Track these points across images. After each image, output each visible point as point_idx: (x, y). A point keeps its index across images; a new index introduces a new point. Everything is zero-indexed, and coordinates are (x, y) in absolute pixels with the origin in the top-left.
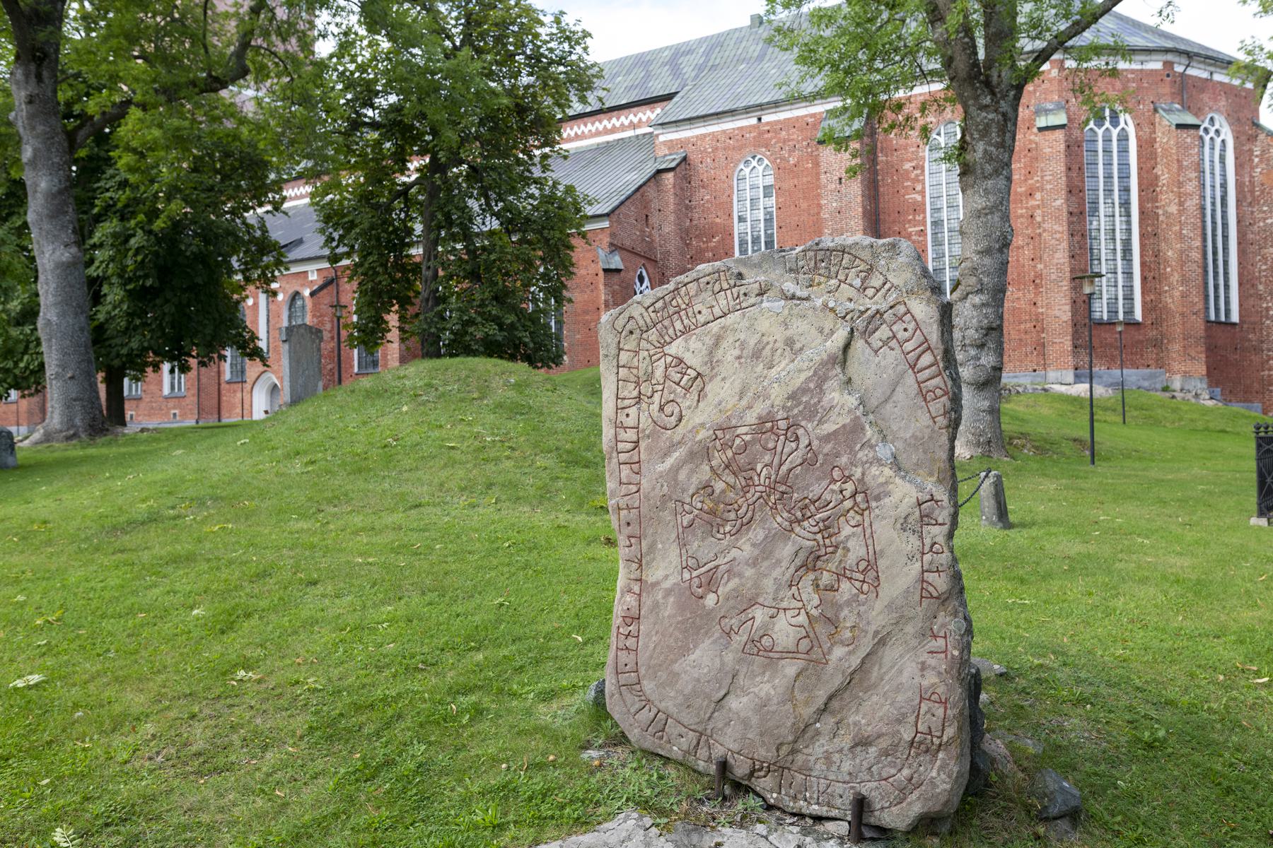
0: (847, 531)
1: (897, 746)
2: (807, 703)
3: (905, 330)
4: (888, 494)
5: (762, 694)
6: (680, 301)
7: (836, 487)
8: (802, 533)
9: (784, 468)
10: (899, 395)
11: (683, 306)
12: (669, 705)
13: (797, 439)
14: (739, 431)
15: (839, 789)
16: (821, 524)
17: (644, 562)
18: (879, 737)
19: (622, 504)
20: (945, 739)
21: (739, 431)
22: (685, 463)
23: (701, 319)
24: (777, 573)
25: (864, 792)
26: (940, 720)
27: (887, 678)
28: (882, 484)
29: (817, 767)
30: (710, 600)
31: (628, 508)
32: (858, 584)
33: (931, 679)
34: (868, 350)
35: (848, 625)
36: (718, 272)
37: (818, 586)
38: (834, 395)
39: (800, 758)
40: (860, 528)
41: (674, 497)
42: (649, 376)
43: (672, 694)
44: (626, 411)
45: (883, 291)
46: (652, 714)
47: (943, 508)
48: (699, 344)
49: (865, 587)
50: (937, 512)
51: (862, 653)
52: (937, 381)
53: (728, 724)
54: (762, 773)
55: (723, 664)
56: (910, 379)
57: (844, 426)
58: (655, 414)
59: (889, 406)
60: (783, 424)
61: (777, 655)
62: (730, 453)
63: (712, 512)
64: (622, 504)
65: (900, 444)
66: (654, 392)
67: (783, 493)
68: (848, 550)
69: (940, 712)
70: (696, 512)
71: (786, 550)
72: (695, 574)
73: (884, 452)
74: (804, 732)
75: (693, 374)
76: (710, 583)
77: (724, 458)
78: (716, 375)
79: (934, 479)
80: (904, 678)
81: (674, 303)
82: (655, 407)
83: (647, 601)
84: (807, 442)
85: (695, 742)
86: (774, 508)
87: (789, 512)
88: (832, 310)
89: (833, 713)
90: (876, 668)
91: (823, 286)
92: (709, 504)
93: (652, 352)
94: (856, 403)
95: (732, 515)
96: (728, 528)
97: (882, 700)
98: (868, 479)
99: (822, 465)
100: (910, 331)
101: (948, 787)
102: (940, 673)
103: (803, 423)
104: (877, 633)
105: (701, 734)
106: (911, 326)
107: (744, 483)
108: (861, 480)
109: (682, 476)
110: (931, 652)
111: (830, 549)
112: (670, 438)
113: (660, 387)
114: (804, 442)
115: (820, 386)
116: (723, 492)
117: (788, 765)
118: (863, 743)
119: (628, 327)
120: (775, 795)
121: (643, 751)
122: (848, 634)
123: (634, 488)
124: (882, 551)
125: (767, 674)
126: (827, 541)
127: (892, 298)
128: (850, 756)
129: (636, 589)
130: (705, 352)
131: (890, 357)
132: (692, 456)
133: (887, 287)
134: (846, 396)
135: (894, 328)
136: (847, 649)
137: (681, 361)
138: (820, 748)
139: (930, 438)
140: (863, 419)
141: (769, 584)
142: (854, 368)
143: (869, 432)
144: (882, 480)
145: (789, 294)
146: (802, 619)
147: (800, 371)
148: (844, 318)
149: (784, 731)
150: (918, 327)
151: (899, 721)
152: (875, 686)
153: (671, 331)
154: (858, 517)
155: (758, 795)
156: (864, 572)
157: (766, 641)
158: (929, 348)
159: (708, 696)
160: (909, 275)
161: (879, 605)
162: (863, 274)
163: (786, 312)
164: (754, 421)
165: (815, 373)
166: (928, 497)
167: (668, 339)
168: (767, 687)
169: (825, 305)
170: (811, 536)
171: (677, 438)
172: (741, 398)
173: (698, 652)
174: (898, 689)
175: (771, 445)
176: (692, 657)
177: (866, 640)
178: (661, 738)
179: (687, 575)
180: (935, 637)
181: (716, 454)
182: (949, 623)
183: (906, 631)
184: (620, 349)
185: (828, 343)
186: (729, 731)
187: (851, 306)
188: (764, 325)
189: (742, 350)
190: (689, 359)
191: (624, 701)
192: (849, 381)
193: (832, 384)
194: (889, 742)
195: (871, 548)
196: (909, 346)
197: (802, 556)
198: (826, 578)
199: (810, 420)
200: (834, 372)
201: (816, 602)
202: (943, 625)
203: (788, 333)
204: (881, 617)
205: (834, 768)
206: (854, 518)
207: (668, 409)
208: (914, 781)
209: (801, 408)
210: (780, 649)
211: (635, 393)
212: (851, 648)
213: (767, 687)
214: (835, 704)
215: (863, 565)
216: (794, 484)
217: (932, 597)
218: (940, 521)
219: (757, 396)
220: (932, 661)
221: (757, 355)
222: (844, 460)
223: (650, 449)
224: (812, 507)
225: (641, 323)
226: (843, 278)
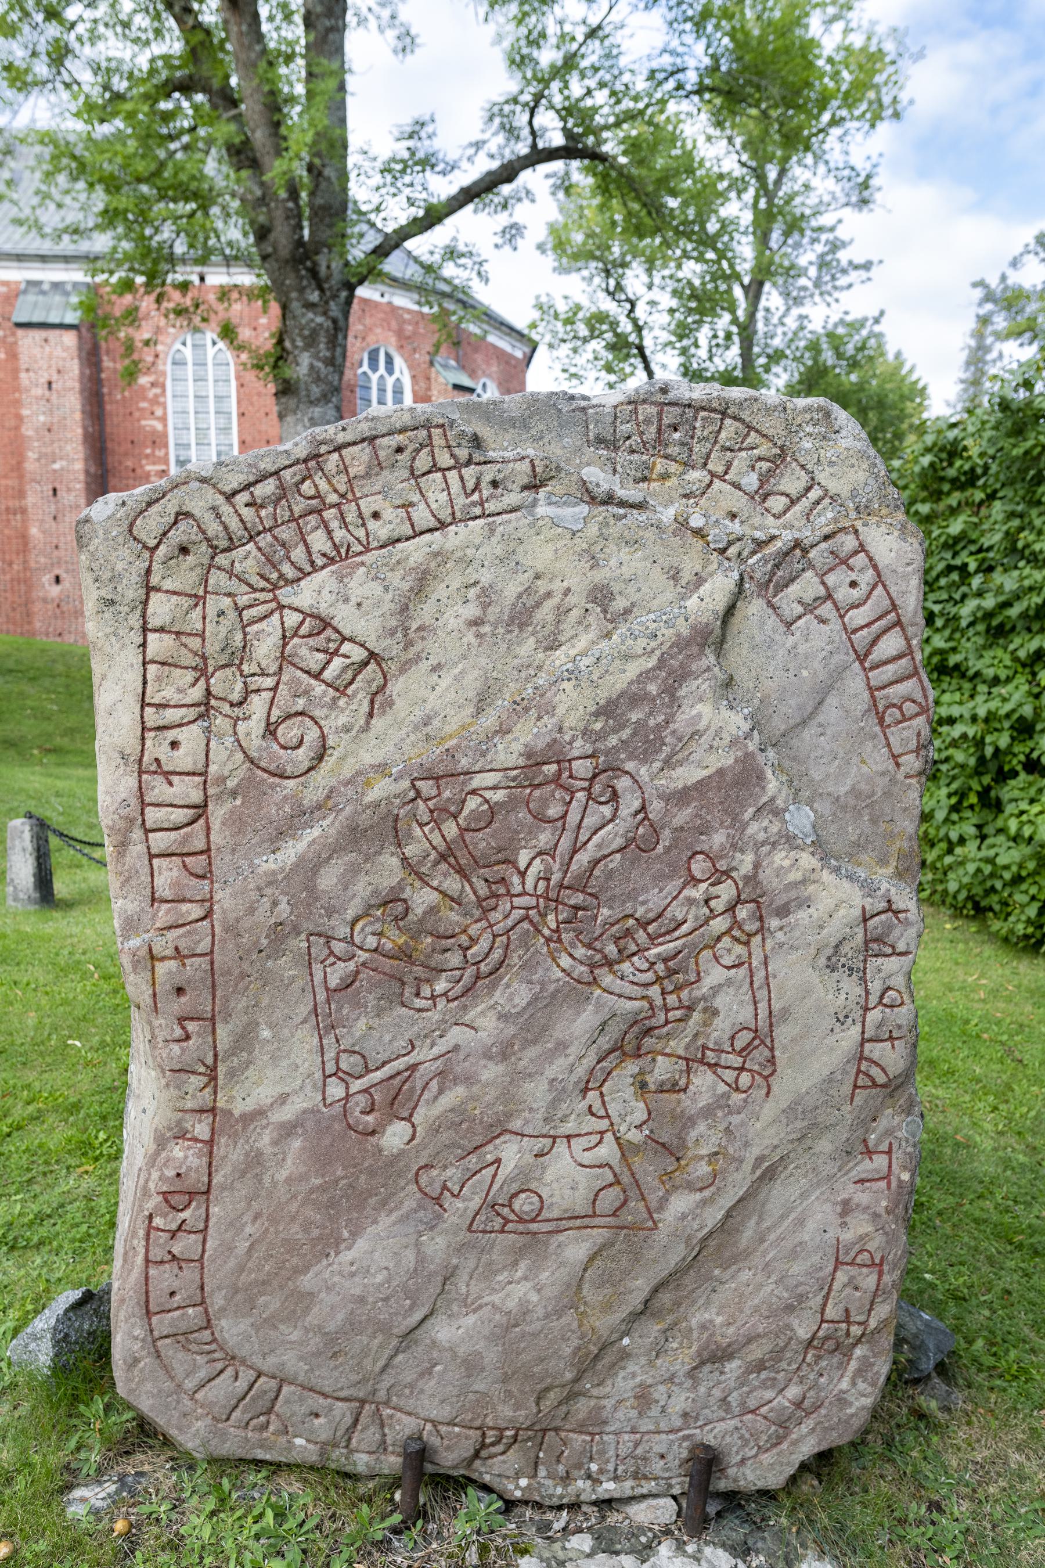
0: (714, 975)
1: (783, 1350)
2: (607, 1307)
3: (853, 584)
4: (806, 903)
5: (511, 1304)
6: (323, 485)
7: (697, 893)
8: (618, 985)
9: (583, 858)
10: (831, 712)
11: (333, 498)
12: (290, 1361)
13: (615, 797)
14: (477, 781)
15: (660, 1443)
16: (660, 967)
17: (221, 1069)
18: (749, 1341)
19: (163, 945)
20: (873, 1323)
21: (477, 781)
22: (336, 850)
23: (380, 530)
24: (556, 1068)
25: (710, 1440)
26: (869, 1296)
27: (772, 1237)
28: (795, 885)
29: (620, 1415)
31: (178, 954)
32: (729, 1075)
33: (860, 1226)
34: (772, 622)
35: (704, 1151)
36: (427, 426)
37: (643, 1085)
38: (700, 709)
39: (582, 1407)
40: (743, 971)
41: (307, 926)
42: (237, 657)
43: (296, 1336)
44: (171, 735)
45: (805, 503)
46: (242, 1385)
47: (907, 923)
48: (377, 588)
49: (745, 1079)
50: (896, 932)
51: (727, 1201)
52: (909, 686)
53: (429, 1372)
54: (500, 1448)
55: (421, 1259)
56: (855, 683)
57: (721, 772)
58: (255, 742)
59: (808, 733)
60: (583, 768)
62: (451, 829)
63: (404, 955)
64: (163, 945)
65: (824, 807)
66: (247, 692)
67: (577, 908)
68: (715, 1013)
69: (869, 1281)
70: (363, 956)
71: (580, 1024)
72: (356, 1085)
73: (801, 819)
74: (597, 1358)
75: (358, 654)
76: (397, 1099)
77: (437, 840)
78: (417, 659)
79: (890, 870)
81: (307, 488)
82: (253, 727)
83: (231, 1154)
84: (637, 804)
85: (348, 1420)
86: (555, 937)
87: (589, 946)
88: (699, 533)
89: (658, 1315)
90: (752, 1223)
91: (673, 482)
92: (395, 938)
93: (243, 601)
94: (746, 726)
95: (455, 959)
96: (441, 986)
97: (761, 1277)
98: (766, 875)
99: (668, 850)
100: (864, 587)
101: (868, 1402)
102: (876, 1216)
103: (629, 766)
104: (760, 1159)
105: (363, 1402)
106: (867, 578)
107: (483, 890)
108: (752, 879)
109: (328, 879)
110: (862, 1181)
111: (678, 1014)
112: (294, 798)
113: (269, 682)
114: (630, 803)
115: (670, 690)
116: (433, 910)
117: (557, 1423)
118: (715, 1356)
119: (176, 536)
120: (523, 1482)
121: (212, 1461)
122: (703, 1169)
123: (196, 911)
124: (785, 1011)
125: (523, 1265)
126: (672, 999)
127: (826, 518)
128: (689, 1383)
129: (201, 1129)
130: (387, 606)
131: (819, 638)
132: (354, 836)
133: (814, 494)
134: (726, 713)
135: (830, 579)
136: (698, 1196)
137: (325, 624)
138: (624, 1383)
139: (887, 794)
140: (761, 759)
141: (536, 1093)
142: (740, 655)
143: (772, 784)
144: (795, 876)
145: (600, 492)
146: (608, 1151)
147: (627, 657)
148: (723, 551)
149: (552, 1365)
150: (879, 579)
151: (790, 1309)
152: (747, 1254)
153: (298, 554)
154: (739, 949)
155: (487, 1488)
156: (745, 1051)
157: (524, 1204)
158: (898, 623)
159: (384, 1328)
160: (862, 476)
161: (770, 1110)
162: (765, 465)
163: (593, 529)
164: (513, 760)
165: (662, 662)
166: (883, 905)
167: (287, 570)
169: (682, 523)
170: (637, 991)
171: (310, 798)
172: (479, 711)
173: (361, 1244)
174: (793, 1255)
175: (553, 811)
176: (347, 1256)
177: (738, 1176)
178: (265, 1426)
179: (336, 1090)
180: (869, 1153)
181: (417, 831)
182: (899, 1127)
183: (817, 1149)
184: (149, 589)
185: (692, 602)
186: (430, 1385)
187: (736, 527)
188: (539, 554)
189: (485, 606)
190: (346, 618)
191: (167, 1370)
192: (729, 683)
193: (699, 686)
194: (768, 1347)
195: (763, 1007)
197: (614, 1031)
198: (663, 1069)
199: (645, 758)
200: (704, 663)
201: (640, 1115)
202: (889, 1132)
203: (599, 576)
204: (772, 1131)
205: (655, 1411)
206: (730, 950)
207: (288, 732)
208: (806, 1404)
209: (625, 734)
210: (555, 1214)
211: (196, 694)
212: (707, 1193)
213: (522, 1289)
214: (666, 1298)
215: (745, 1037)
216: (603, 889)
217: (875, 1085)
218: (901, 947)
219: (520, 707)
220: (862, 1197)
221: (520, 618)
222: (718, 839)
223: (237, 823)
224: (641, 936)
225: (213, 528)
226: (720, 469)
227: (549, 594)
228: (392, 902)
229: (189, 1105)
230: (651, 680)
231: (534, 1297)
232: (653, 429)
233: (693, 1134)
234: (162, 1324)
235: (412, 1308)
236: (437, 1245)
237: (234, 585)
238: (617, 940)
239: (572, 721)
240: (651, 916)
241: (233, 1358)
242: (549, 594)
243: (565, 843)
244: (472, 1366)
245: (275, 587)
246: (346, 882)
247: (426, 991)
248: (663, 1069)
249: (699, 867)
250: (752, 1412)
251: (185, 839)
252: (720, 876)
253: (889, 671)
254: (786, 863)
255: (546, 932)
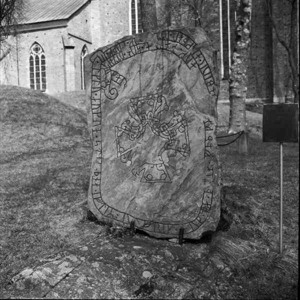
0: (179, 134)
2: (164, 198)
4: (193, 120)
10: (198, 84)
11: (118, 52)
13: (161, 101)
14: (140, 99)
21: (140, 99)
23: (125, 57)
28: (191, 116)
30: (129, 163)
32: (182, 153)
44: (95, 93)
51: (183, 178)
55: (133, 187)
61: (153, 182)
76: (129, 156)
80: (198, 186)
83: (104, 166)
104: (189, 170)
106: (202, 59)
107: (141, 118)
109: (117, 117)
114: (164, 102)
116: (133, 122)
123: (99, 123)
135: (197, 60)
136: (179, 177)
141: (150, 156)
146: (163, 168)
151: (196, 201)
153: (113, 62)
156: (185, 149)
161: (190, 160)
166: (207, 120)
167: (112, 64)
168: (149, 194)
171: (115, 103)
176: (122, 185)
179: (119, 155)
180: (209, 170)
184: (93, 69)
196: (201, 66)
198: (172, 152)
206: (182, 129)
207: (112, 92)
210: (154, 179)
222: (178, 108)
228: (127, 121)
229: (98, 157)
231: (152, 195)
233: (177, 165)
234: (95, 196)
235: (132, 196)
236: (136, 184)
237: (105, 68)
238: (163, 127)
241: (105, 204)
242: (151, 66)
243: (154, 110)
244: (142, 208)
245: (110, 67)
246: (120, 117)
247: (133, 137)
248: (172, 152)
250: (192, 222)
251: (97, 111)
253: (207, 76)
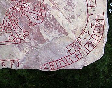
0: (8, 35)
4: (21, 50)
8: (6, 19)
9: (28, 14)
10: (53, 55)
38: (54, 33)
40: (9, 40)
56: (56, 58)
60: (43, 14)
99: (29, 28)
100: (72, 59)
106: (74, 60)
108: (24, 42)
114: (38, 22)
144: (25, 49)
175: (36, 9)
196: (68, 59)
199: (45, 24)
203: (76, 17)
222: (31, 36)
227: (73, 8)
230: (58, 25)
232: (100, 26)
239: (51, 12)
240: (18, 25)
242: (73, 8)
243: (31, 11)
249: (26, 33)
252: (25, 36)
253: (58, 64)
254: (27, 47)
255: (15, 7)
